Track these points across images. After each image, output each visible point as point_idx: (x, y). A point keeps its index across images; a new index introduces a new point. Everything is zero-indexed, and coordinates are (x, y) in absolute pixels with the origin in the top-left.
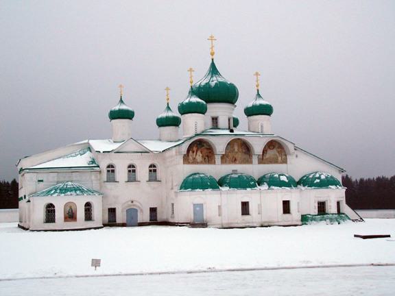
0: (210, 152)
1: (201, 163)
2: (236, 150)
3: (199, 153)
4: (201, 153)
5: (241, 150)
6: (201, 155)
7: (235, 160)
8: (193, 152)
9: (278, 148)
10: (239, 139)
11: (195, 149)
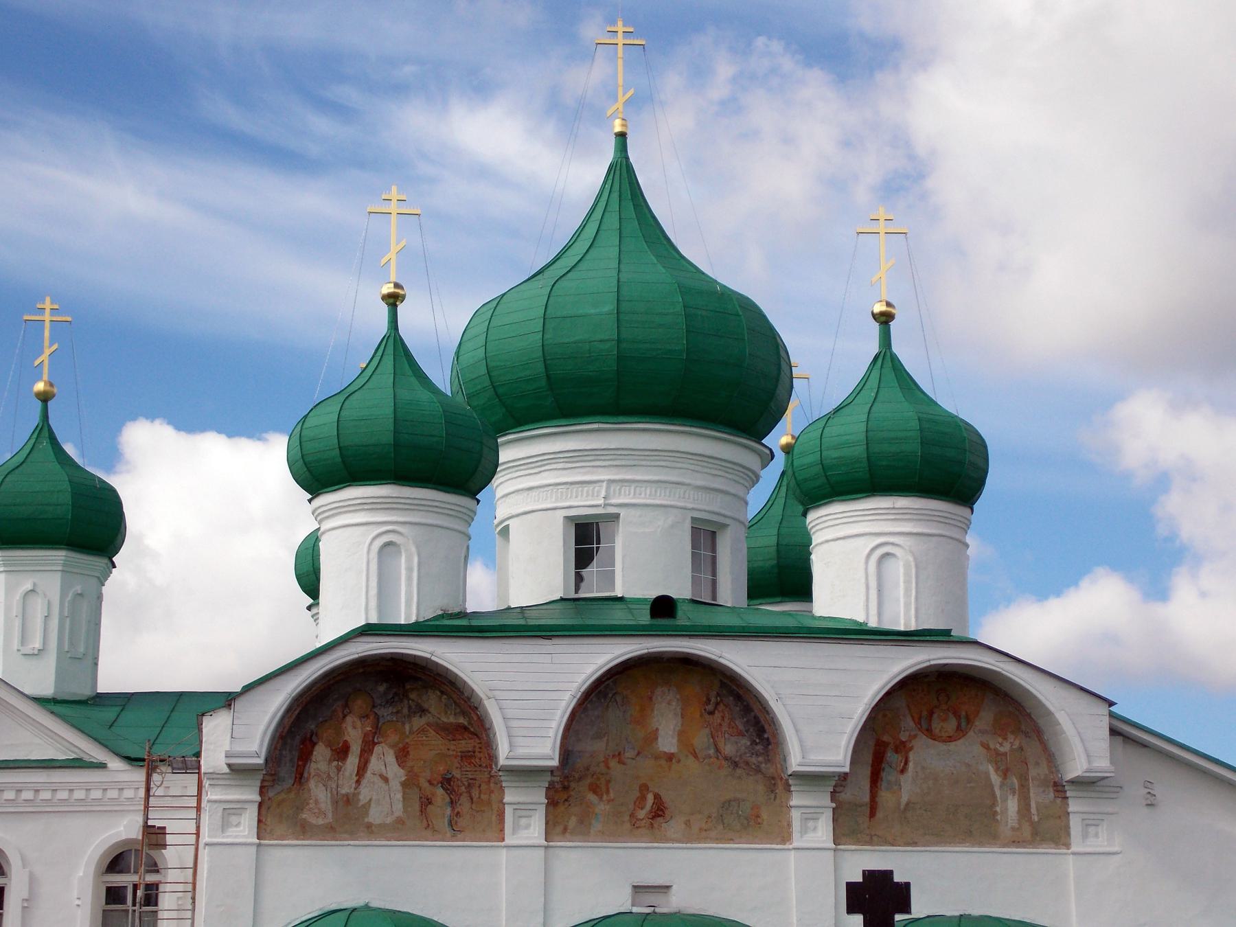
0: (467, 756)
1: (397, 830)
2: (667, 742)
3: (384, 760)
4: (402, 755)
5: (701, 739)
6: (396, 773)
7: (659, 811)
8: (342, 752)
9: (1000, 729)
10: (688, 663)
11: (353, 732)
